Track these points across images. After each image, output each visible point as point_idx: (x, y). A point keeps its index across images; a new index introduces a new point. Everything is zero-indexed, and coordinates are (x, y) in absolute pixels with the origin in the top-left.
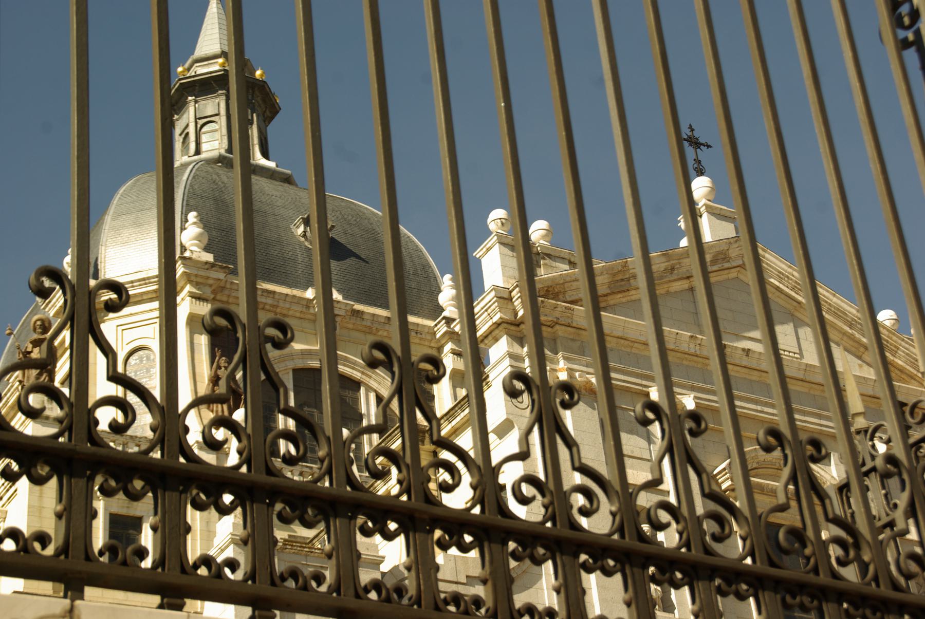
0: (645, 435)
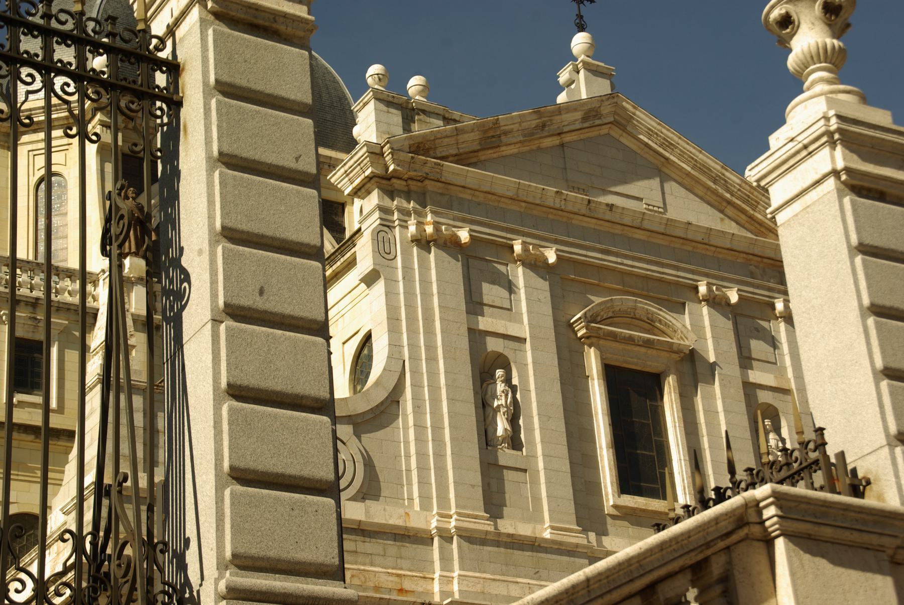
0: (507, 285)
